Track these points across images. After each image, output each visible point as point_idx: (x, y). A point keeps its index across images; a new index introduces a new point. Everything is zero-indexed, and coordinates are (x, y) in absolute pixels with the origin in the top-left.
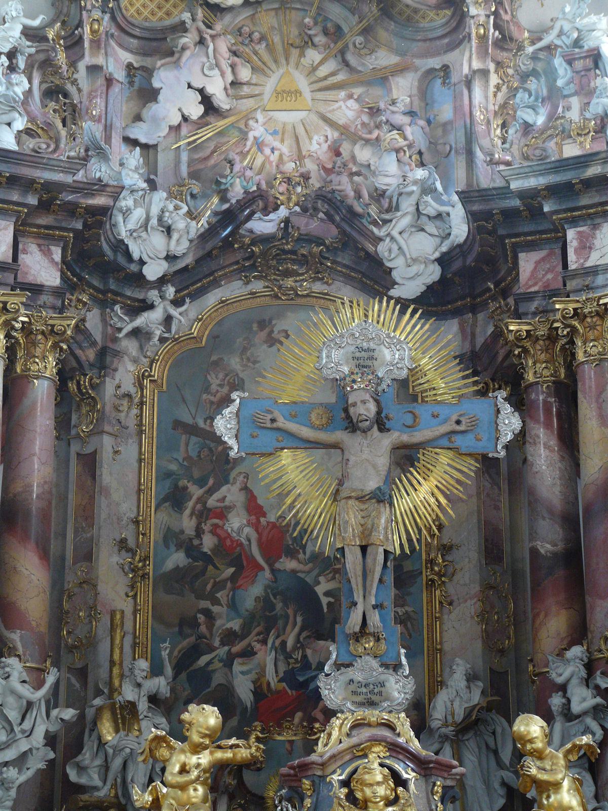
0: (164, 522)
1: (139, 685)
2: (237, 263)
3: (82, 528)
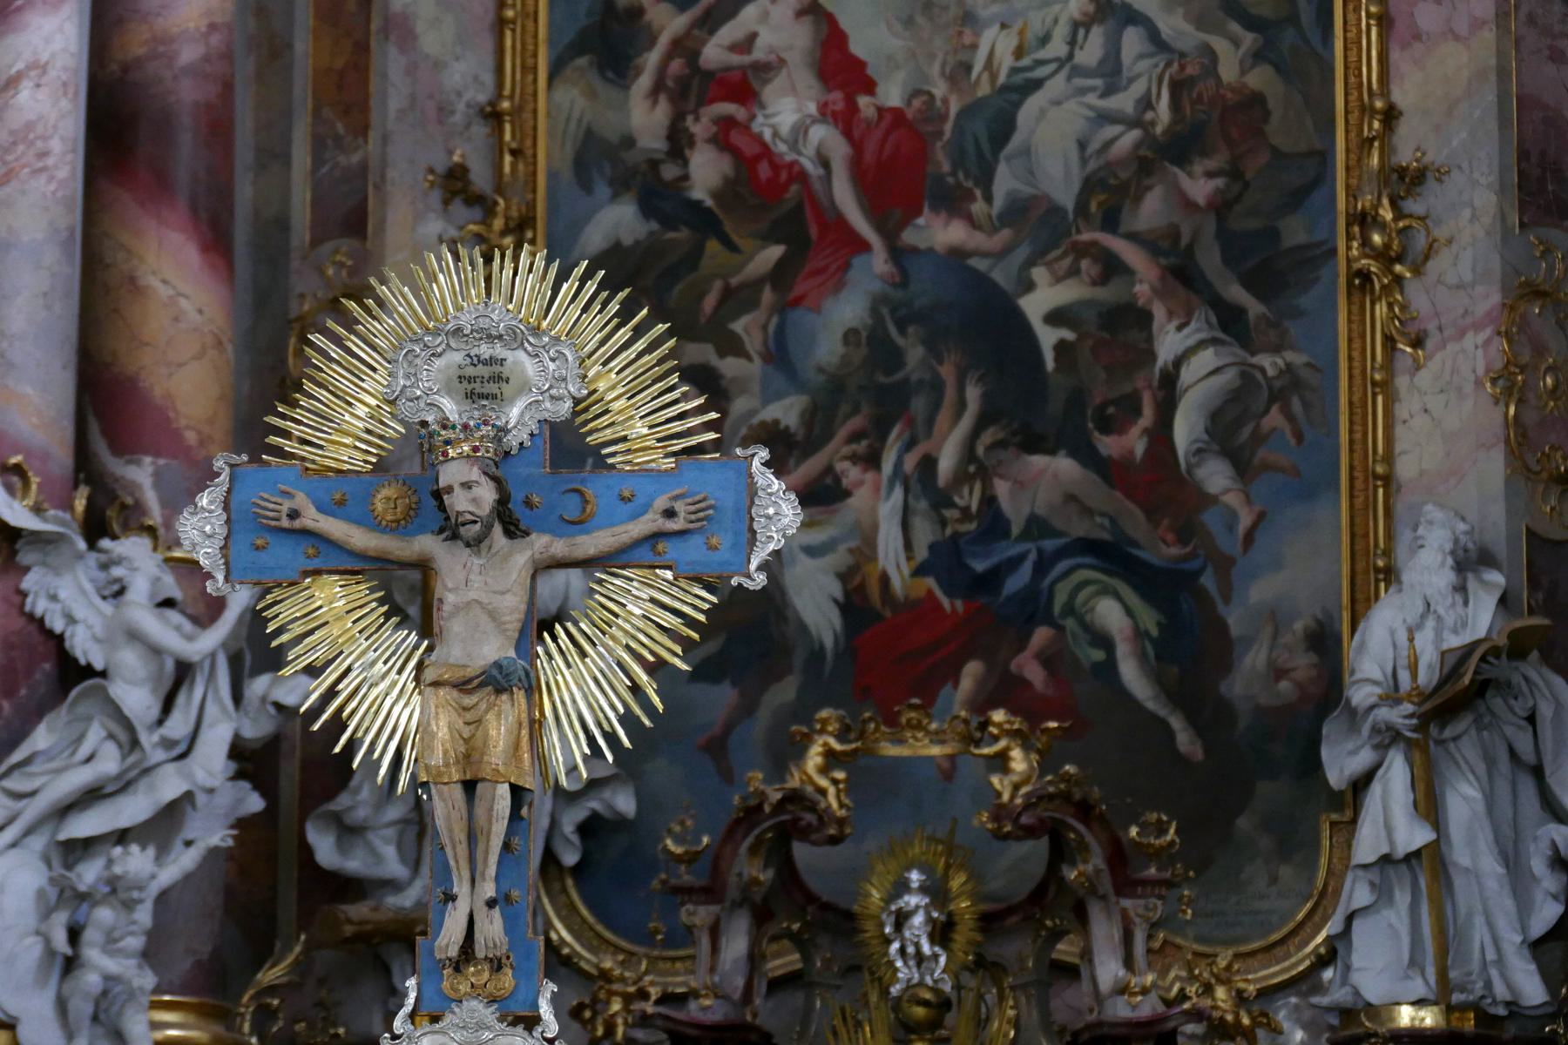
0: (576, 114)
3: (337, 139)
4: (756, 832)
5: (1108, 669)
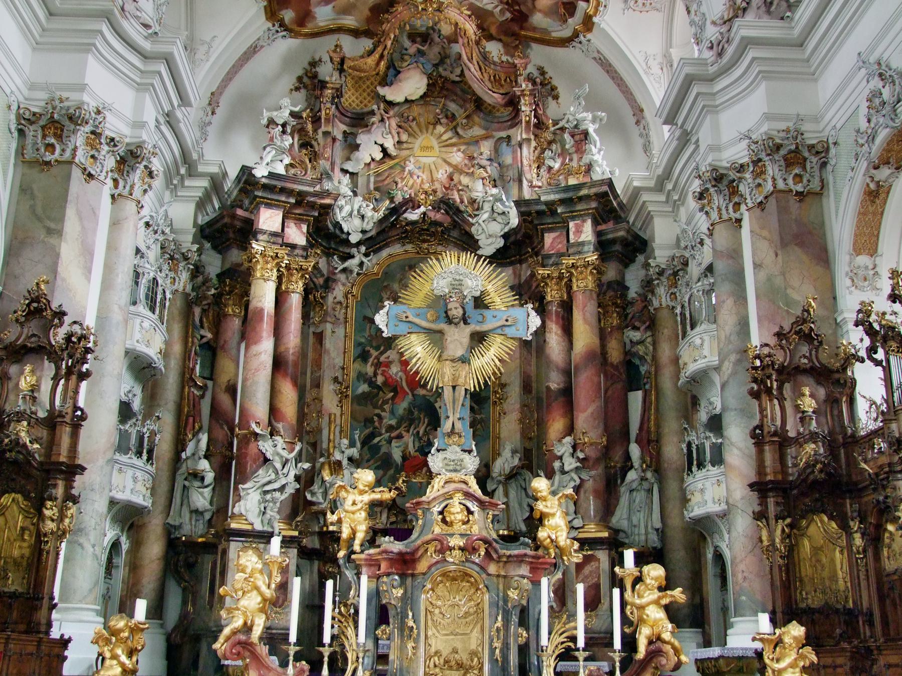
1: (343, 452)
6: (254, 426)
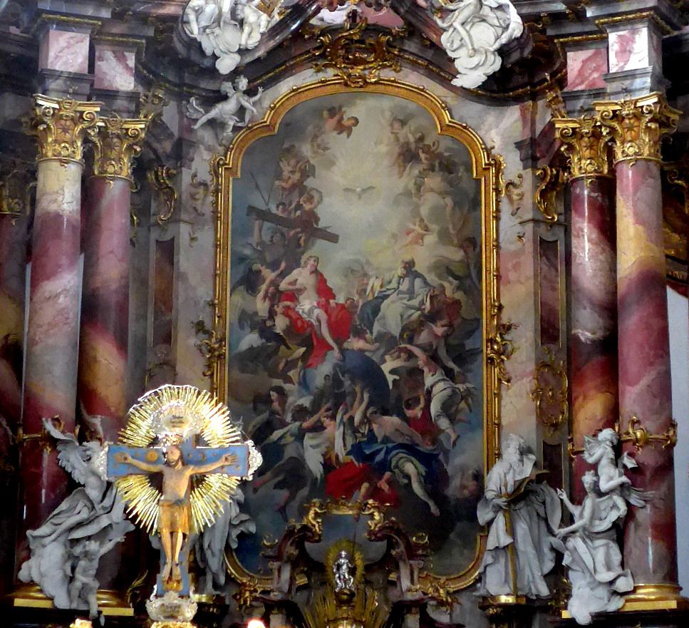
0: (239, 305)
2: (308, 52)
3: (162, 312)
4: (292, 539)
5: (409, 485)
6: (49, 426)
